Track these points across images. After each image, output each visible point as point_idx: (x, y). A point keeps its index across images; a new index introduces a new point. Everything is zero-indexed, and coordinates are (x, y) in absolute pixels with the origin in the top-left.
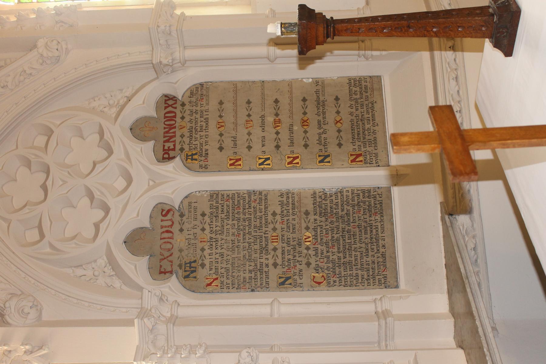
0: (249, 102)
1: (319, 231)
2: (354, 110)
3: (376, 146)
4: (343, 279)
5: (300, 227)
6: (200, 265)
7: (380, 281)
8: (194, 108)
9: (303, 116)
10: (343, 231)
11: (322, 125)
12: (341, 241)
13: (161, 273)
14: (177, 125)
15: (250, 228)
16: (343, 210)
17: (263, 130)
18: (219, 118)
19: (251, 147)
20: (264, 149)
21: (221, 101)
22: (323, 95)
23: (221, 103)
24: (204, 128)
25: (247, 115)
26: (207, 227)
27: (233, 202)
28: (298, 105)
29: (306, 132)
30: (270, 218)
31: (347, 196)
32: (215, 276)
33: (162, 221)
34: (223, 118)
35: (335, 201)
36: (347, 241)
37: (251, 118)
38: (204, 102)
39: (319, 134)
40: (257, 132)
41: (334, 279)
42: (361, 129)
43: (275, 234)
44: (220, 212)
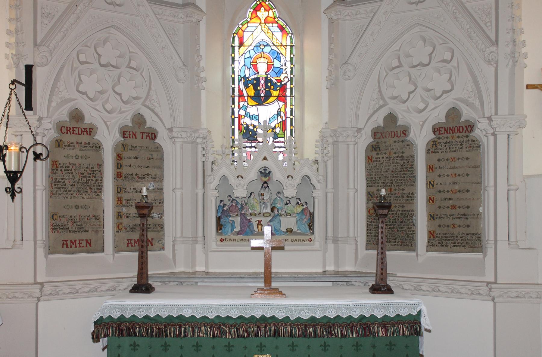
0: (468, 175)
1: (394, 212)
2: (461, 235)
3: (439, 246)
4: (371, 223)
5: (396, 203)
6: (378, 153)
7: (370, 241)
8: (464, 143)
9: (458, 206)
10: (393, 225)
11: (452, 217)
12: (389, 224)
13: (375, 133)
14: (455, 134)
15: (396, 177)
16: (404, 225)
17: (450, 184)
18: (457, 158)
19: (440, 177)
20: (439, 184)
21: (469, 159)
22: (471, 218)
23: (467, 159)
24: (452, 150)
25: (459, 174)
26: (397, 155)
27: (409, 168)
28: (465, 203)
29: (448, 207)
30: (401, 188)
31: (411, 228)
32: (373, 160)
33: (400, 131)
34: (458, 160)
35: (409, 221)
36: (389, 227)
37: (458, 176)
38: (468, 149)
39: (446, 215)
40: (449, 180)
41: (371, 219)
42: (449, 238)
43: (393, 190)
44: (404, 161)
